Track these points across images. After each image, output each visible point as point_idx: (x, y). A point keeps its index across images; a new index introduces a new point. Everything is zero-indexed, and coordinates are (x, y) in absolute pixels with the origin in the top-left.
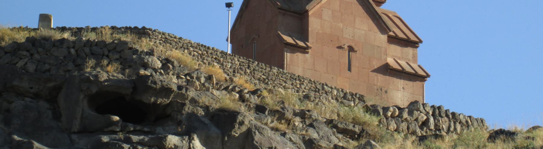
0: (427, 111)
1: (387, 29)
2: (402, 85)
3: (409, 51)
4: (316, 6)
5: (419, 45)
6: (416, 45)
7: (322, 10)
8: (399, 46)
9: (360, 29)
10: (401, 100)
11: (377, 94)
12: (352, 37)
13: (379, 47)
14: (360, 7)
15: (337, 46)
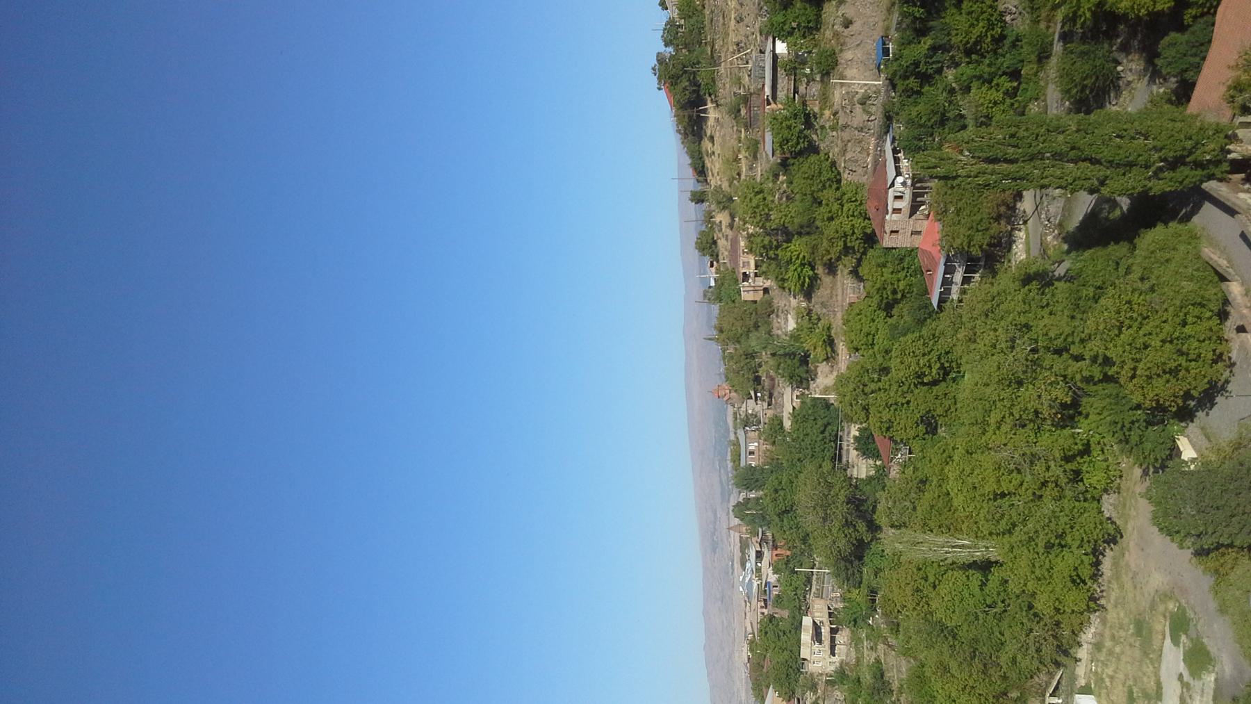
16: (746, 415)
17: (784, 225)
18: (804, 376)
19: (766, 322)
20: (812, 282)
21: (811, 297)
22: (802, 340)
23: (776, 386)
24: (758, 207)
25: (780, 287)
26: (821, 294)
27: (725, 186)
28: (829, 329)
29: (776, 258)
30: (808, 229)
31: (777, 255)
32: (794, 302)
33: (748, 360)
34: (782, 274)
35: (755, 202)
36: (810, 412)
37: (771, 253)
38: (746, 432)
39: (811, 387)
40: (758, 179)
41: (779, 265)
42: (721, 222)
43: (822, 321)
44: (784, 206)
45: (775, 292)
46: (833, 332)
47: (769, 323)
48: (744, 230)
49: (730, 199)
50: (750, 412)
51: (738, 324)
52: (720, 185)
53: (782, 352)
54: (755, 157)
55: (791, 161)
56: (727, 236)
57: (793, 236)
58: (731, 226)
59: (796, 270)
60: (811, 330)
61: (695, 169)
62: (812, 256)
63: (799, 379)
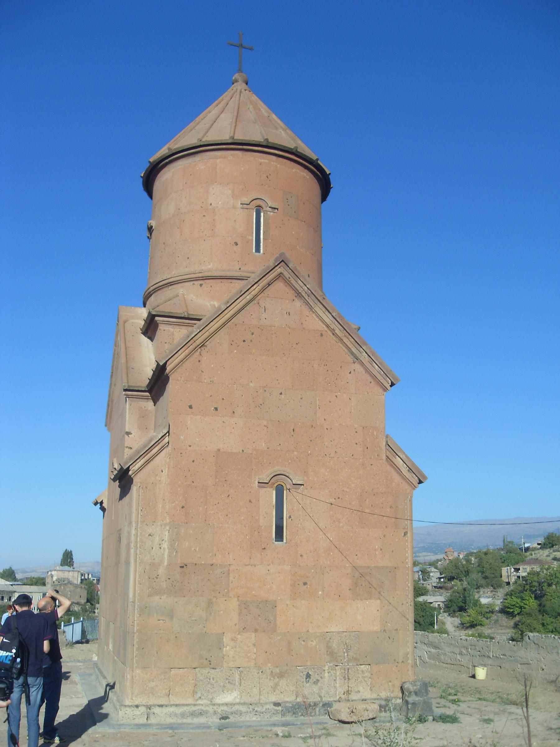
16: (429, 572)
17: (545, 594)
18: (452, 609)
20: (510, 613)
21: (501, 613)
22: (474, 607)
23: (447, 591)
26: (504, 620)
28: (481, 625)
30: (542, 610)
31: (526, 591)
32: (498, 602)
33: (464, 573)
34: (515, 594)
36: (428, 613)
38: (418, 572)
39: (445, 614)
41: (521, 592)
43: (486, 620)
45: (507, 589)
46: (479, 627)
47: (487, 586)
50: (431, 574)
53: (467, 595)
56: (549, 556)
57: (539, 601)
60: (481, 613)
62: (525, 614)
63: (450, 606)
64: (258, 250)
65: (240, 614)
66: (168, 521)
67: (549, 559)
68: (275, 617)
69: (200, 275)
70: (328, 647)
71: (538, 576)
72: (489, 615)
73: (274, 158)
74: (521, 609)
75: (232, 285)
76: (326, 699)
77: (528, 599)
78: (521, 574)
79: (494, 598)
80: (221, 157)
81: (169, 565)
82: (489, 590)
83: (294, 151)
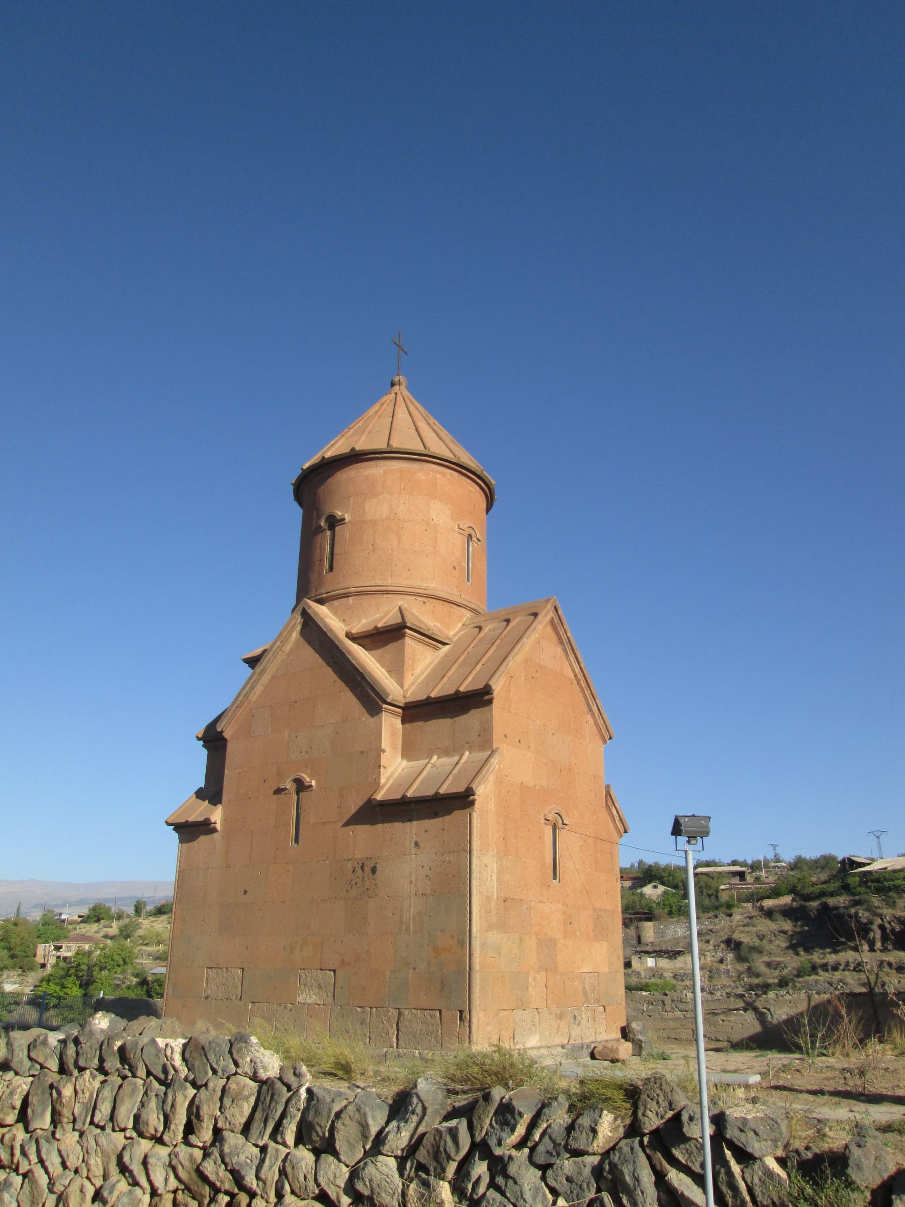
0: (41, 1060)
1: (378, 700)
2: (414, 836)
3: (473, 717)
4: (239, 713)
5: (492, 694)
6: (486, 697)
7: (253, 716)
8: (445, 717)
9: (323, 726)
10: (411, 883)
11: (353, 883)
12: (307, 752)
13: (362, 753)
14: (329, 670)
15: (275, 788)
19: (15, 965)
21: (30, 1005)
24: (113, 960)
25: (43, 978)
27: (140, 932)
29: (68, 975)
31: (70, 976)
32: (28, 990)
34: (54, 980)
35: (116, 957)
37: (72, 971)
40: (137, 961)
41: (62, 977)
42: (111, 927)
44: (111, 982)
48: (95, 948)
49: (127, 937)
51: (18, 940)
52: (141, 928)
54: (157, 958)
55: (145, 988)
58: (106, 936)
59: (56, 992)
61: (163, 906)
64: (468, 580)
65: (537, 951)
66: (496, 851)
67: (99, 935)
68: (556, 955)
69: (426, 592)
70: (584, 988)
71: (89, 957)
72: (13, 1007)
73: (478, 488)
74: (59, 1001)
75: (452, 610)
76: (586, 1041)
77: (70, 986)
78: (63, 953)
79: (21, 983)
80: (440, 473)
81: (497, 898)
82: (16, 973)
83: (492, 487)
